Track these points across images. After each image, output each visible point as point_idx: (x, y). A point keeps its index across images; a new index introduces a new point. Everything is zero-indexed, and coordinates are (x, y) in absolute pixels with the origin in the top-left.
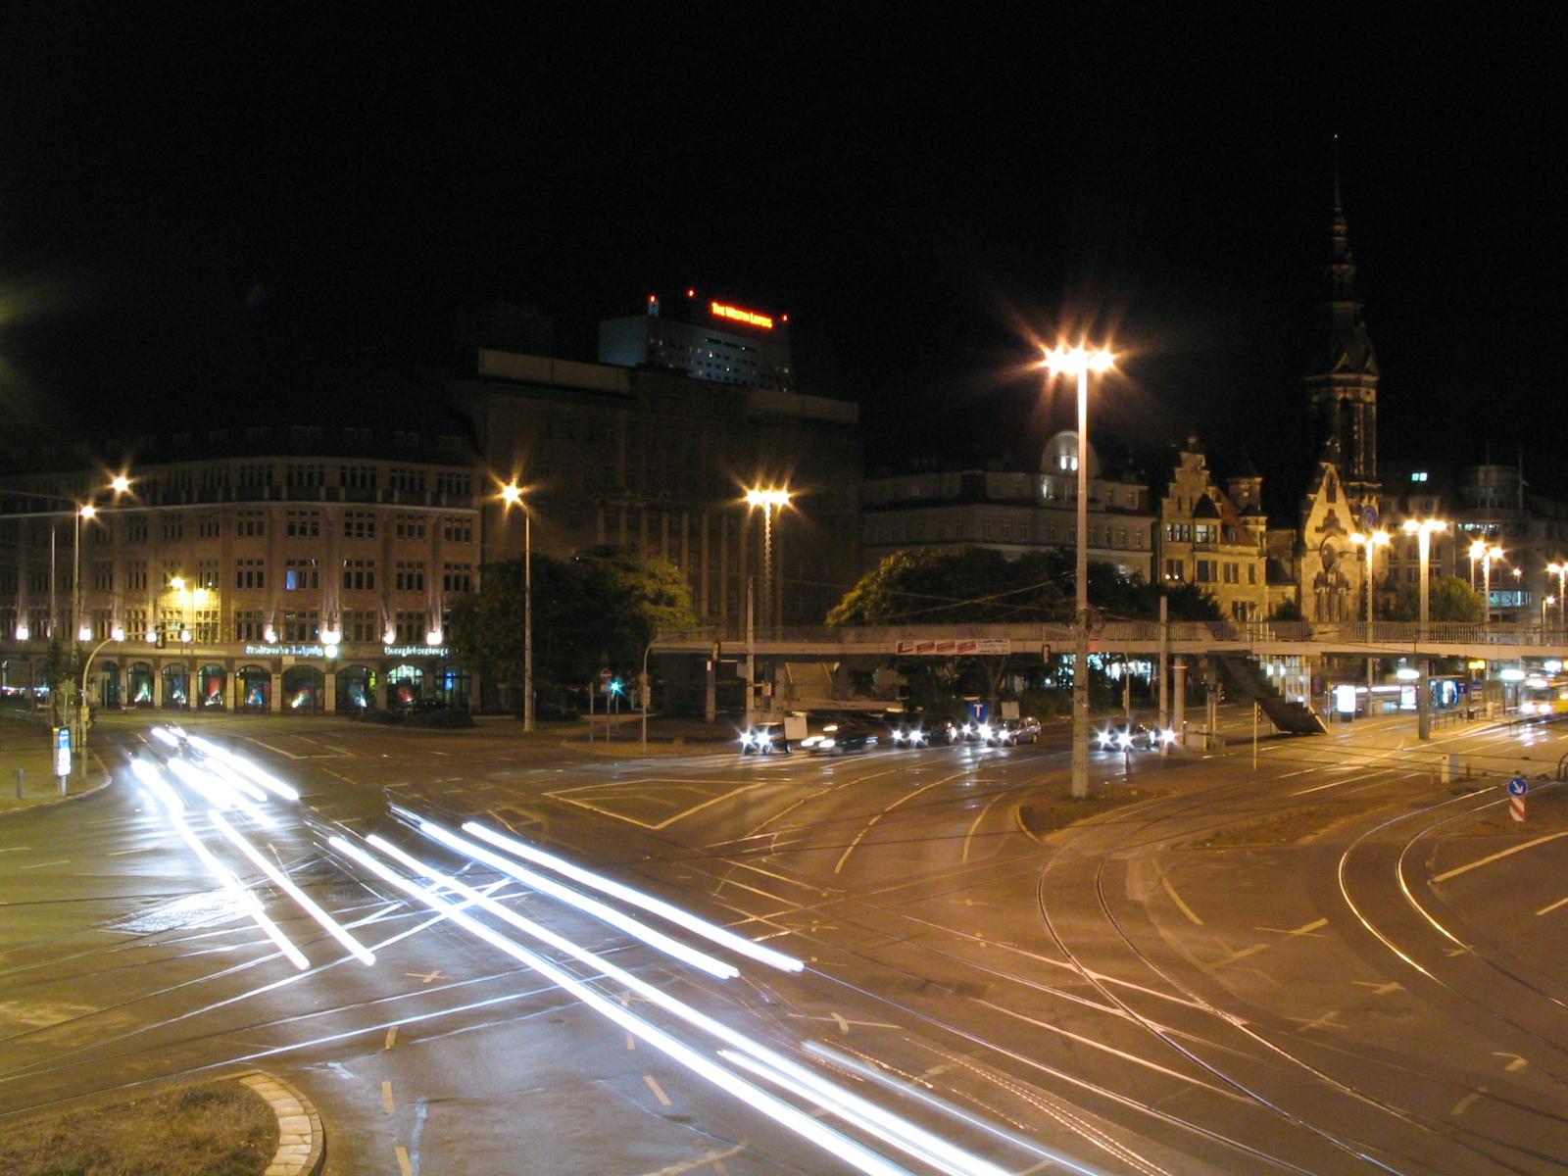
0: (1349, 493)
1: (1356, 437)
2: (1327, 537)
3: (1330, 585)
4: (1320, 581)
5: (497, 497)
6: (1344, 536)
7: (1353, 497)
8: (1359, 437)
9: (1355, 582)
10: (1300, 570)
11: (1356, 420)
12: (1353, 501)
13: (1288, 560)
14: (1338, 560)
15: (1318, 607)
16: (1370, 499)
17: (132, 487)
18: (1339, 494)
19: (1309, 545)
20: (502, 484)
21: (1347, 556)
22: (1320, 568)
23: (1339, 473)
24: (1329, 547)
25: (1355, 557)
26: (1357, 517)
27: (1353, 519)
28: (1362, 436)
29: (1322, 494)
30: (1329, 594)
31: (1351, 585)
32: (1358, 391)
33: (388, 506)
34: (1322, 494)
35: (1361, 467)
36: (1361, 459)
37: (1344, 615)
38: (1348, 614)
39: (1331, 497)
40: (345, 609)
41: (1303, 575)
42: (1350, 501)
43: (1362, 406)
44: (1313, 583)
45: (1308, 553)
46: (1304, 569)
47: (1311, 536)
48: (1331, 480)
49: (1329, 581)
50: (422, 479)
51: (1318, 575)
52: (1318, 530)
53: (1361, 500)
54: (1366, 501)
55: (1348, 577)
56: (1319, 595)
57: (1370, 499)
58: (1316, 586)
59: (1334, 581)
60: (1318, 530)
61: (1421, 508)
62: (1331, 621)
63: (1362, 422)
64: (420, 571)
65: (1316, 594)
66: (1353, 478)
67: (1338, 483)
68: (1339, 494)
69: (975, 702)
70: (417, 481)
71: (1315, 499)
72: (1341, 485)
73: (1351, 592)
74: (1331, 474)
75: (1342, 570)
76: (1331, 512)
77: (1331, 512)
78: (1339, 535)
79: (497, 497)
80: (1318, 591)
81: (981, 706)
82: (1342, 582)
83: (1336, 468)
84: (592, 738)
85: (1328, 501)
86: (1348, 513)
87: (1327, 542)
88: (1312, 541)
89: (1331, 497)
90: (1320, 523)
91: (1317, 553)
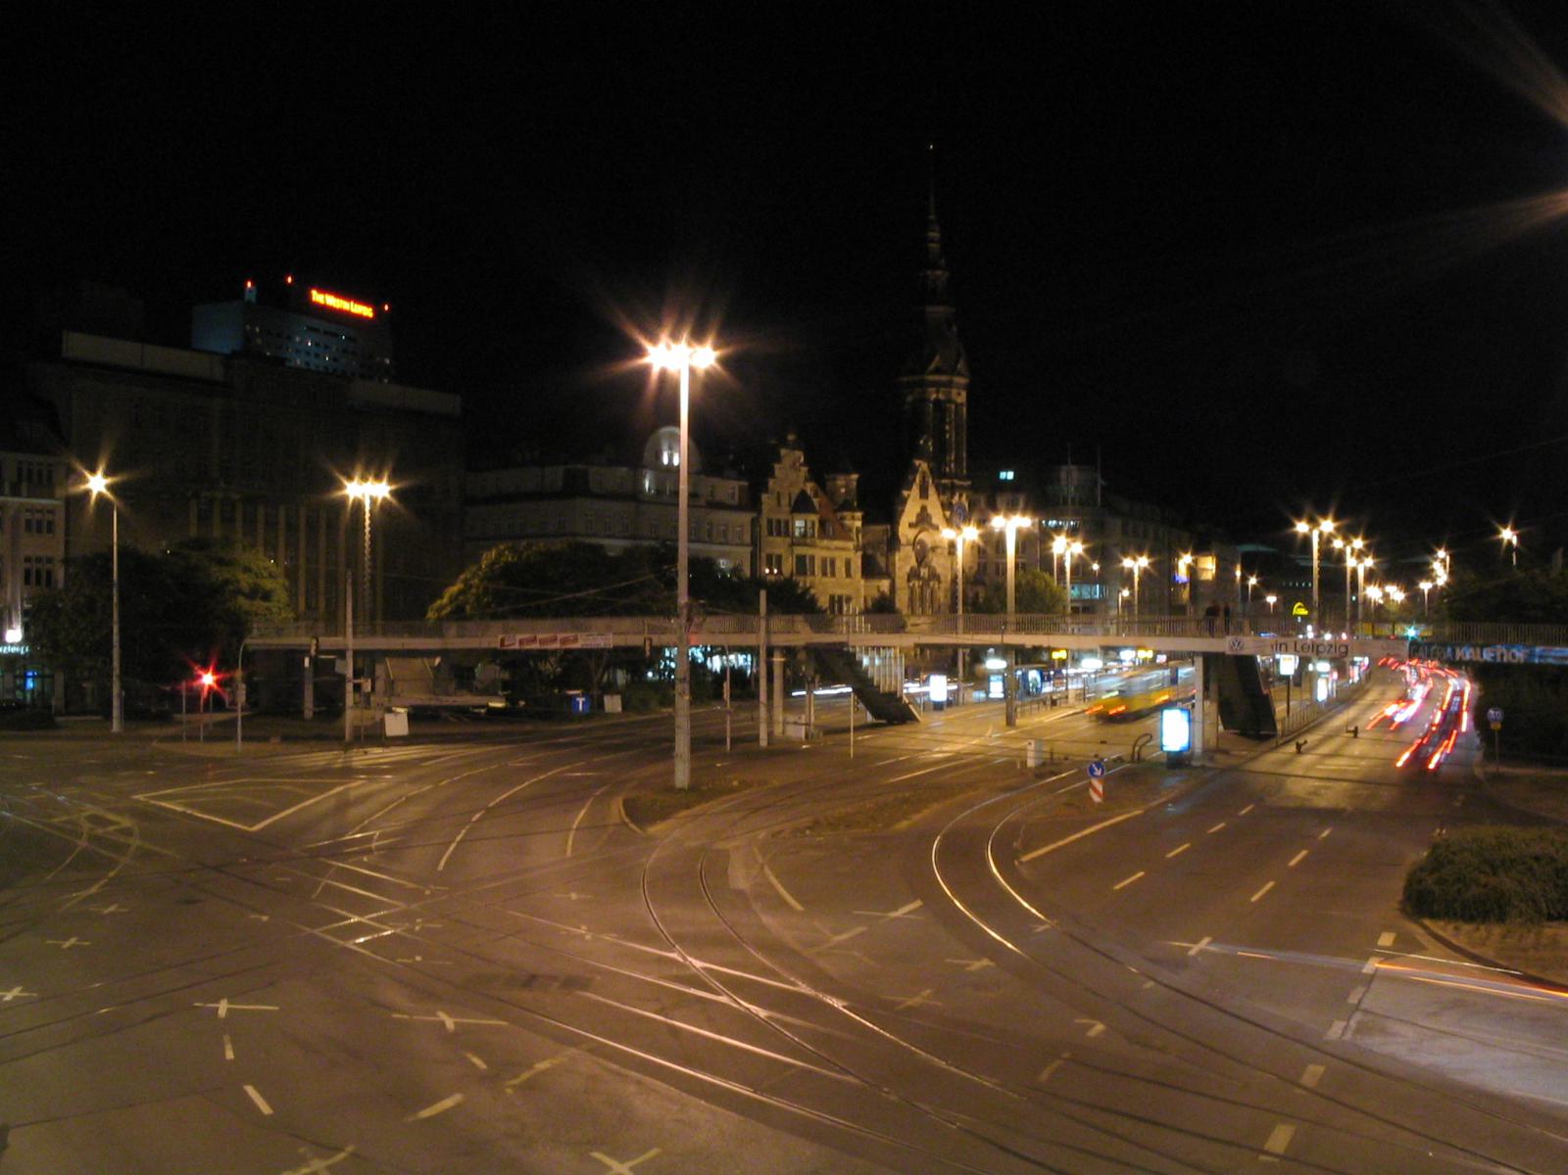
0: (941, 490)
1: (948, 436)
2: (920, 532)
3: (923, 578)
4: (913, 575)
5: (340, 493)
6: (934, 533)
7: (944, 493)
8: (950, 437)
9: (946, 576)
10: (894, 565)
11: (948, 420)
12: (944, 498)
13: (882, 555)
14: (930, 555)
15: (911, 600)
16: (961, 496)
17: (1499, 533)
18: (932, 491)
19: (903, 540)
20: (393, 487)
21: (939, 551)
22: (914, 563)
23: (932, 471)
24: (922, 543)
25: (946, 552)
26: (948, 513)
27: (944, 515)
28: (954, 435)
29: (915, 490)
30: (922, 588)
31: (942, 578)
32: (950, 393)
33: (16, 499)
34: (915, 490)
35: (952, 465)
36: (953, 458)
37: (936, 606)
38: (939, 607)
39: (924, 494)
40: (26, 606)
41: (897, 570)
42: (942, 497)
43: (953, 407)
44: (906, 577)
45: (902, 548)
46: (898, 564)
47: (905, 532)
48: (924, 478)
49: (922, 574)
50: (50, 472)
51: (912, 568)
52: (911, 525)
53: (952, 498)
54: (956, 498)
55: (939, 570)
56: (912, 590)
57: (961, 496)
58: (909, 580)
59: (926, 575)
60: (911, 525)
61: (1008, 504)
62: (923, 613)
63: (953, 423)
64: (49, 566)
65: (909, 587)
66: (945, 476)
67: (930, 481)
68: (932, 491)
69: (578, 696)
70: (45, 473)
71: (909, 496)
72: (933, 482)
73: (943, 586)
74: (924, 472)
75: (934, 564)
76: (924, 509)
77: (924, 509)
78: (931, 530)
79: (340, 493)
80: (911, 584)
81: (584, 699)
82: (934, 576)
83: (929, 466)
84: (362, 737)
85: (921, 497)
86: (940, 510)
87: (919, 537)
88: (906, 536)
89: (924, 494)
90: (913, 519)
91: (910, 548)
